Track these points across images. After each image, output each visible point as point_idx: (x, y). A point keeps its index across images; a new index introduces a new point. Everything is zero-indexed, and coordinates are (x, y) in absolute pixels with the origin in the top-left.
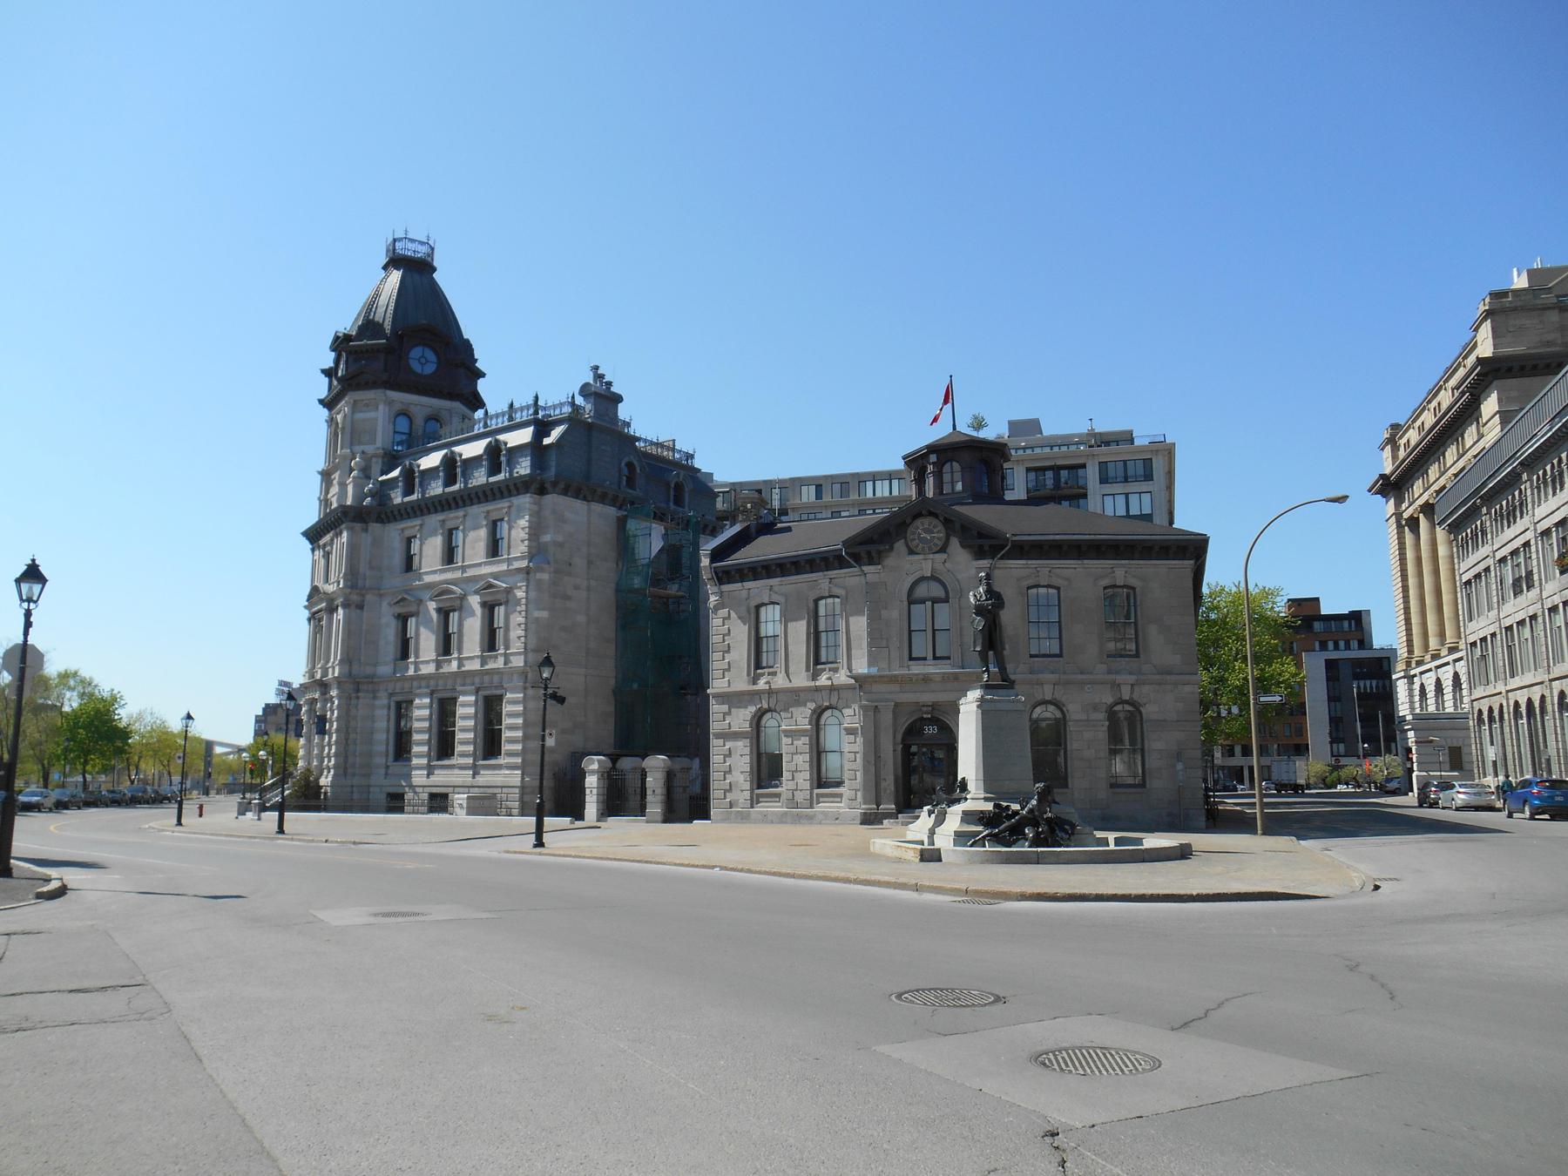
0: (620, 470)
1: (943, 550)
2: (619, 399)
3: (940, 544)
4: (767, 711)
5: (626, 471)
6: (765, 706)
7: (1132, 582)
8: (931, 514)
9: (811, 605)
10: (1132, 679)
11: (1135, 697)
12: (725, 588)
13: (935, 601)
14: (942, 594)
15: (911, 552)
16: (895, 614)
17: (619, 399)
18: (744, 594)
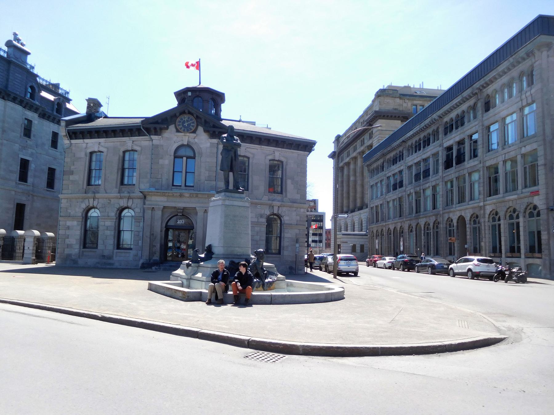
0: (26, 89)
1: (194, 132)
2: (28, 53)
3: (193, 129)
4: (93, 207)
5: (30, 90)
6: (91, 205)
7: (282, 159)
8: (190, 113)
9: (121, 154)
10: (278, 204)
11: (280, 212)
12: (73, 141)
13: (188, 158)
14: (191, 154)
15: (178, 131)
16: (166, 162)
17: (28, 53)
18: (84, 145)
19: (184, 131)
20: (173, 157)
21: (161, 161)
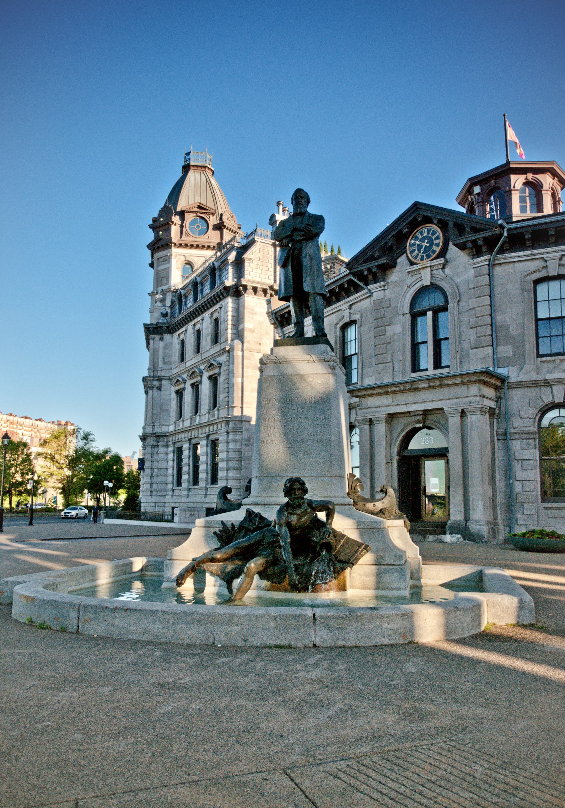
3: (438, 249)
14: (441, 302)
16: (398, 328)
19: (422, 259)
20: (408, 317)
21: (390, 331)
